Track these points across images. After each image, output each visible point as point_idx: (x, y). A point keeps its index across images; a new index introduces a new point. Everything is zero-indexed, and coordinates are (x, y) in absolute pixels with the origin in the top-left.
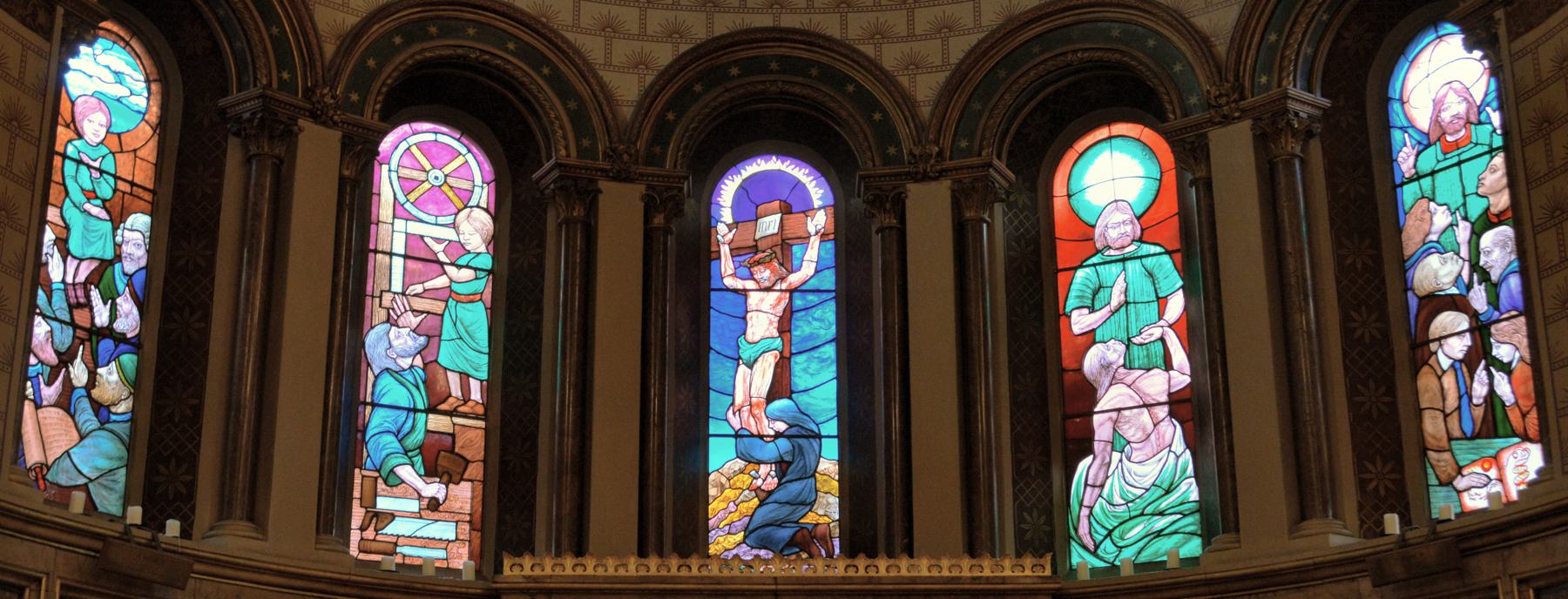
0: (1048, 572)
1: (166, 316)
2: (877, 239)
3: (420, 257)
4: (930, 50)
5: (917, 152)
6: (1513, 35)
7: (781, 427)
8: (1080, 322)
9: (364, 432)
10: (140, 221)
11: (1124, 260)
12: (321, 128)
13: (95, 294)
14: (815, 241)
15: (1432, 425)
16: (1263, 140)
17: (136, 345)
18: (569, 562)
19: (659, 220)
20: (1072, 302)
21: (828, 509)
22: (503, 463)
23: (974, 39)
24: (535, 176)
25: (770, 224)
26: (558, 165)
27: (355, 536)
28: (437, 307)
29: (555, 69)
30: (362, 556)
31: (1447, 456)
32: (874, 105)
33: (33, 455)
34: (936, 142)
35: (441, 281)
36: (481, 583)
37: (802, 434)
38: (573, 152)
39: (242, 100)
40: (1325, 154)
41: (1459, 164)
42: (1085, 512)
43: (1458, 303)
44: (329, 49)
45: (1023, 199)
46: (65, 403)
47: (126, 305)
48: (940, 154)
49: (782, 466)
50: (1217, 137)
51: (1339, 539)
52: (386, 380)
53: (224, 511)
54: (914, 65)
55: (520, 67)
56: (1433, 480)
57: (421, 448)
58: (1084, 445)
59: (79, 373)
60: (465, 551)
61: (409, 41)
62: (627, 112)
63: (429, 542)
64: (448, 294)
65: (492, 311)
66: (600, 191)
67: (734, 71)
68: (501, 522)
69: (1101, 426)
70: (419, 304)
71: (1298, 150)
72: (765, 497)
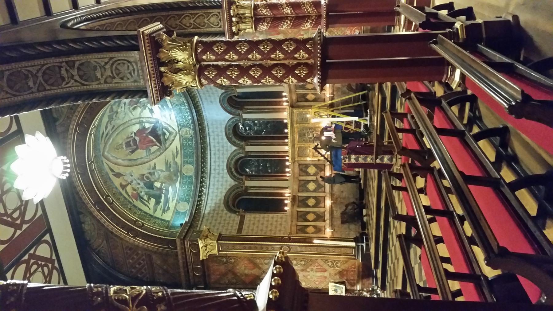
44: (236, 183)
62: (237, 148)
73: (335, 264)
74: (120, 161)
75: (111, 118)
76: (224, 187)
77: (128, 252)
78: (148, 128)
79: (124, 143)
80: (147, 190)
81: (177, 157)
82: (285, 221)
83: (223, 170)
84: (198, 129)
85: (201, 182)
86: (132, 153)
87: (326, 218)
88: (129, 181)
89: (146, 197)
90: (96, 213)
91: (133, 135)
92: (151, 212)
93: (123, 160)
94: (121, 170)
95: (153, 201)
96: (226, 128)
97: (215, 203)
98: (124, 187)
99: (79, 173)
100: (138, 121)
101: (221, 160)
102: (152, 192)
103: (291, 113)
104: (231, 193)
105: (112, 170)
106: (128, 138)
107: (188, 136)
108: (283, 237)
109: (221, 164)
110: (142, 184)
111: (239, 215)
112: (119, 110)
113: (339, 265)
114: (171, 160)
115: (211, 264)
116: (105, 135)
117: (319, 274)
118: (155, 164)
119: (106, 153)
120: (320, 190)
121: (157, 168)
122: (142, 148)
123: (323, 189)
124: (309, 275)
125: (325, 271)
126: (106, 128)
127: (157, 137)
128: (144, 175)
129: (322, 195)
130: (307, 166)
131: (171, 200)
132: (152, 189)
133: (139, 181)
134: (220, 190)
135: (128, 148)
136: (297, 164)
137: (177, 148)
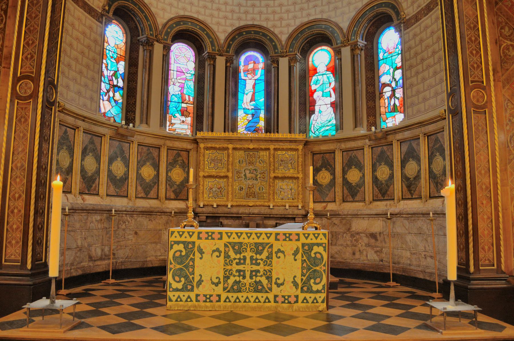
0: (305, 137)
1: (128, 83)
2: (273, 69)
3: (181, 72)
4: (285, 30)
5: (282, 51)
6: (405, 30)
7: (253, 107)
8: (313, 88)
9: (169, 107)
10: (122, 63)
11: (323, 75)
12: (159, 44)
13: (114, 78)
14: (260, 69)
15: (382, 110)
16: (352, 50)
17: (122, 88)
18: (210, 133)
19: (228, 64)
20: (312, 83)
21: (262, 124)
22: (197, 114)
23: (294, 28)
24: (203, 55)
25: (251, 66)
26: (208, 52)
27: (168, 128)
28: (183, 82)
29: (207, 32)
30: (169, 132)
31: (385, 116)
32: (273, 41)
33: (103, 111)
34: (286, 49)
35: (184, 77)
36: (193, 137)
38: (211, 50)
39: (142, 38)
40: (365, 53)
41: (392, 56)
42: (313, 125)
43: (389, 85)
44: (160, 27)
45: (303, 62)
46: (109, 100)
47: (120, 80)
48: (286, 52)
49: (253, 115)
50: (343, 49)
51: (362, 131)
52: (173, 96)
53: (141, 122)
54: (281, 33)
55: (200, 32)
56: (382, 121)
57: (180, 110)
58: (312, 112)
59: (111, 94)
60: (189, 131)
61: (177, 26)
62: (222, 42)
63: (182, 129)
64: (185, 79)
65: (194, 82)
66: (216, 58)
67: (244, 33)
68: (197, 125)
69: (317, 108)
70: (180, 81)
71: (359, 53)
72: (249, 121)
82: (85, 105)
83: (184, 9)
87: (86, 197)
96: (260, 27)
101: (202, 10)
108: (56, 87)
109: (194, 9)
120: (139, 188)
123: (143, 195)
130: (186, 167)
136: (189, 146)
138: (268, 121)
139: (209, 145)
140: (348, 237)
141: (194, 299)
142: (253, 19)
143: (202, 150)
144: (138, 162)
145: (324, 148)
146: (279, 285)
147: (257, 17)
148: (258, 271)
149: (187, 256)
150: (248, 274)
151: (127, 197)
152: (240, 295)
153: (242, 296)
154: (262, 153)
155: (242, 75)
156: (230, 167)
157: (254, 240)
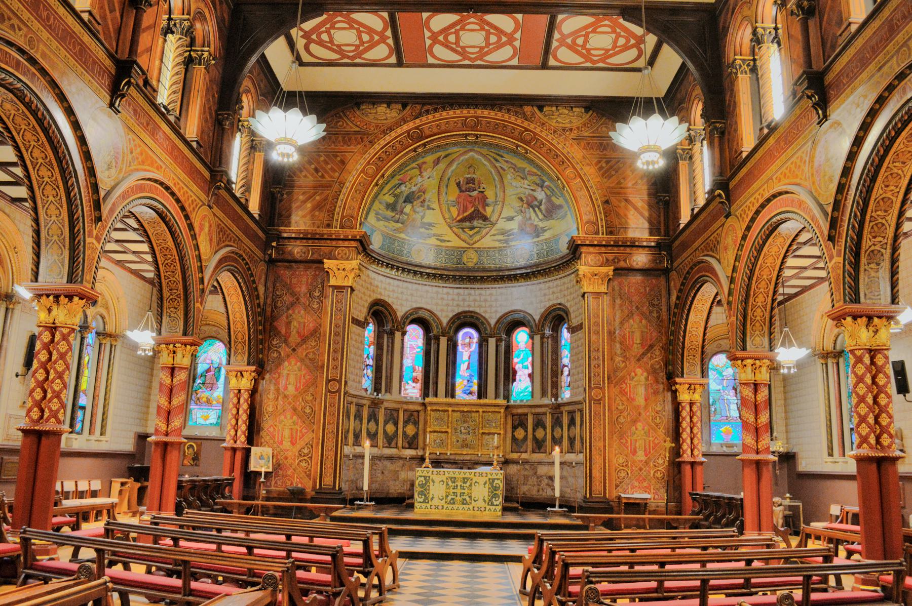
3: (412, 348)
4: (494, 315)
10: (372, 347)
14: (475, 344)
15: (563, 384)
16: (542, 338)
21: (475, 388)
25: (467, 340)
37: (471, 376)
39: (387, 328)
43: (567, 366)
47: (371, 360)
49: (468, 381)
50: (535, 336)
51: (546, 401)
54: (491, 317)
58: (514, 380)
59: (365, 372)
62: (445, 325)
69: (518, 377)
72: (465, 386)
73: (305, 458)
74: (454, 166)
75: (515, 168)
76: (395, 301)
77: (339, 159)
78: (485, 210)
79: (474, 176)
80: (405, 195)
81: (438, 239)
84: (476, 275)
85: (403, 269)
86: (457, 184)
87: (356, 447)
88: (424, 174)
89: (399, 190)
90: (405, 128)
91: (481, 190)
92: (380, 197)
93: (452, 172)
94: (442, 166)
95: (390, 199)
96: (474, 312)
97: (377, 287)
98: (420, 167)
99: (466, 120)
100: (500, 198)
102: (401, 200)
103: (498, 406)
104: (388, 310)
105: (446, 156)
106: (479, 183)
107: (465, 259)
110: (414, 189)
111: (366, 319)
112: (526, 182)
113: (304, 464)
114: (435, 231)
115: (311, 273)
116: (498, 158)
117: (287, 433)
118: (433, 209)
119: (471, 153)
120: (385, 440)
121: (428, 212)
122: (459, 197)
123: (387, 445)
124: (285, 417)
125: (293, 444)
126: (507, 162)
127: (470, 218)
128: (424, 193)
129: (380, 443)
130: (416, 423)
131: (387, 224)
132: (405, 202)
133: (418, 186)
134: (391, 294)
135: (466, 180)
137: (448, 241)
138: (480, 386)
139: (434, 408)
140: (535, 479)
141: (429, 508)
142: (469, 306)
143: (429, 412)
144: (385, 421)
145: (520, 411)
146: (475, 501)
147: (472, 304)
148: (464, 493)
149: (426, 484)
150: (459, 495)
151: (377, 446)
152: (454, 506)
153: (455, 506)
154: (473, 414)
155: (460, 348)
156: (450, 425)
157: (462, 475)
